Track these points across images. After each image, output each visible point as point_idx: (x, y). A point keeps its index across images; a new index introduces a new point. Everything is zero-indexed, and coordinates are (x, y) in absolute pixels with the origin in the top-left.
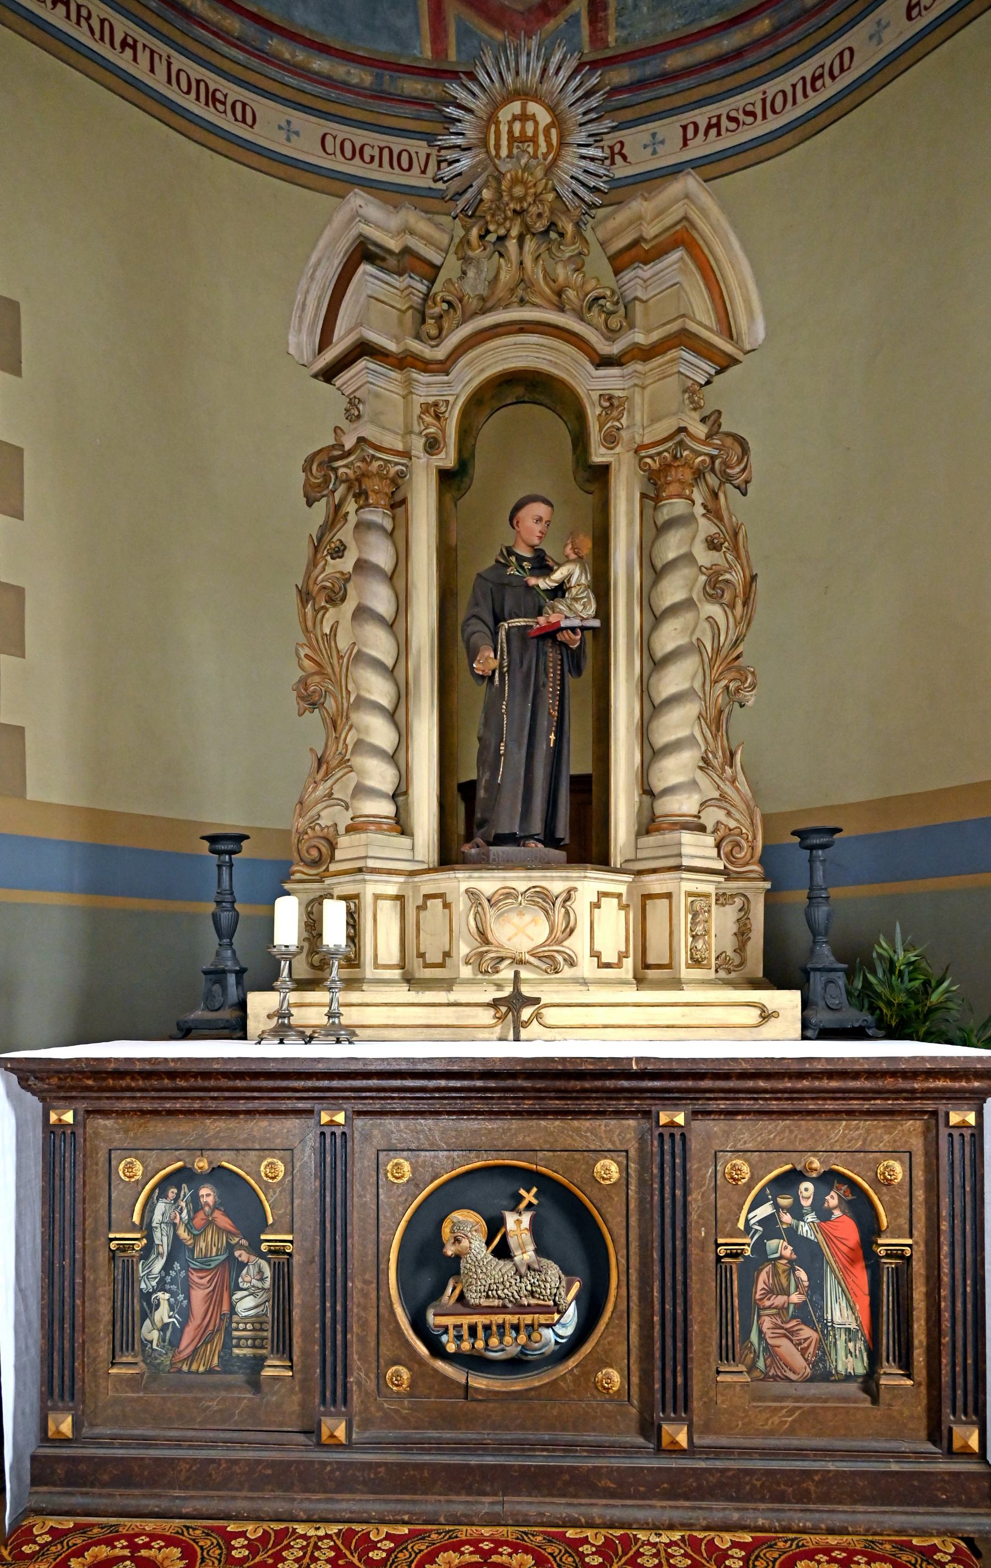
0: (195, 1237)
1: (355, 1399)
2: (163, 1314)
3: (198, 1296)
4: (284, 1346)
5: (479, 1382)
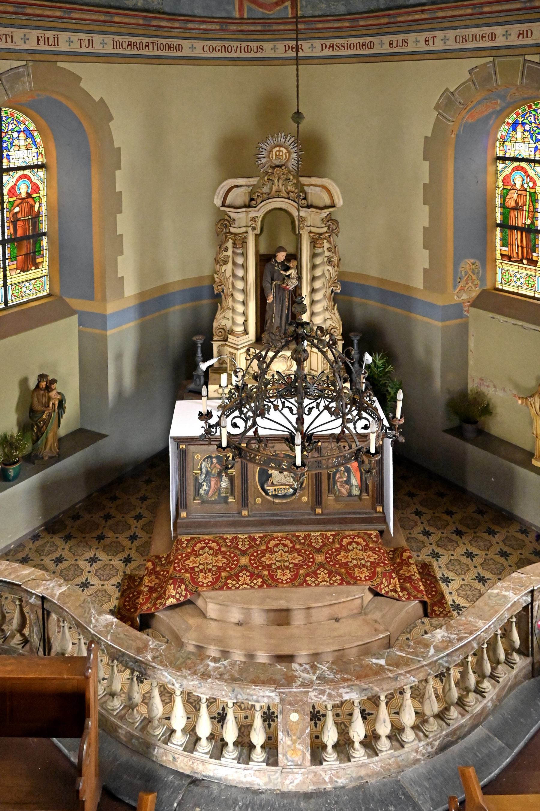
0: (212, 470)
1: (249, 505)
2: (205, 487)
3: (213, 483)
4: (232, 493)
5: (276, 501)
